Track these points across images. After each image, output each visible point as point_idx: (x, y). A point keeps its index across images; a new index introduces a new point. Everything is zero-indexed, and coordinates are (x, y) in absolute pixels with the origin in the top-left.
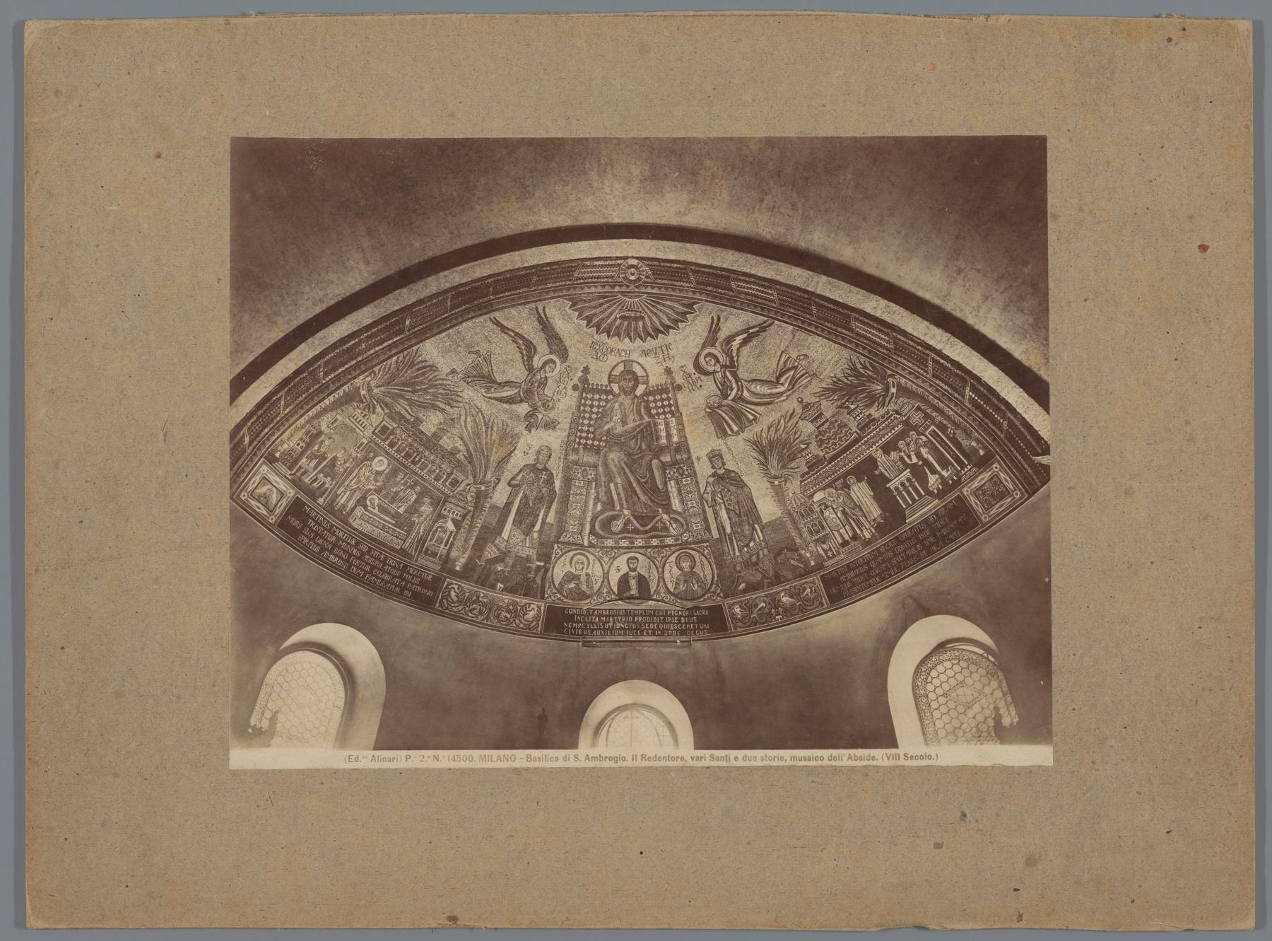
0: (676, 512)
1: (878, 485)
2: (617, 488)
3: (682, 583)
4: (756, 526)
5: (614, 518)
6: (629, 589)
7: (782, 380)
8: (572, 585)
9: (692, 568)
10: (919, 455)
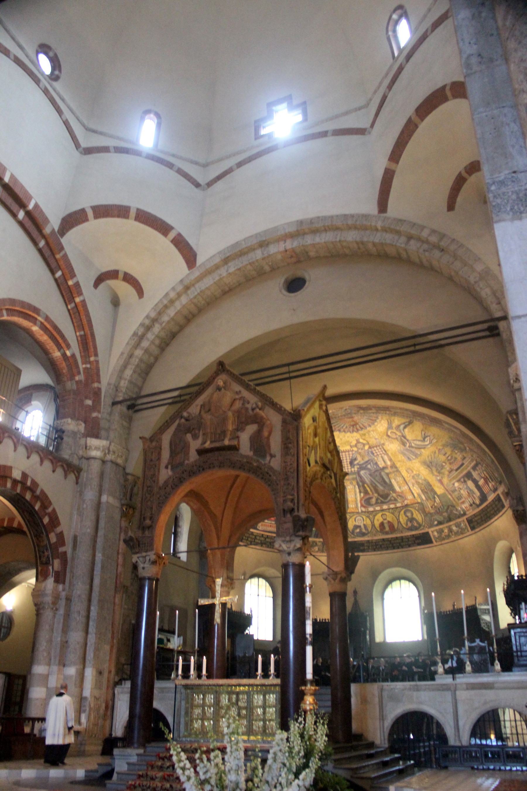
0: (399, 492)
1: (475, 482)
2: (368, 486)
3: (409, 523)
4: (436, 496)
5: (371, 498)
6: (384, 528)
7: (426, 440)
8: (358, 530)
9: (412, 514)
10: (485, 475)
